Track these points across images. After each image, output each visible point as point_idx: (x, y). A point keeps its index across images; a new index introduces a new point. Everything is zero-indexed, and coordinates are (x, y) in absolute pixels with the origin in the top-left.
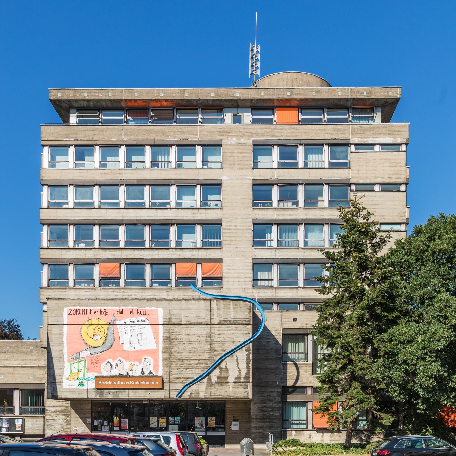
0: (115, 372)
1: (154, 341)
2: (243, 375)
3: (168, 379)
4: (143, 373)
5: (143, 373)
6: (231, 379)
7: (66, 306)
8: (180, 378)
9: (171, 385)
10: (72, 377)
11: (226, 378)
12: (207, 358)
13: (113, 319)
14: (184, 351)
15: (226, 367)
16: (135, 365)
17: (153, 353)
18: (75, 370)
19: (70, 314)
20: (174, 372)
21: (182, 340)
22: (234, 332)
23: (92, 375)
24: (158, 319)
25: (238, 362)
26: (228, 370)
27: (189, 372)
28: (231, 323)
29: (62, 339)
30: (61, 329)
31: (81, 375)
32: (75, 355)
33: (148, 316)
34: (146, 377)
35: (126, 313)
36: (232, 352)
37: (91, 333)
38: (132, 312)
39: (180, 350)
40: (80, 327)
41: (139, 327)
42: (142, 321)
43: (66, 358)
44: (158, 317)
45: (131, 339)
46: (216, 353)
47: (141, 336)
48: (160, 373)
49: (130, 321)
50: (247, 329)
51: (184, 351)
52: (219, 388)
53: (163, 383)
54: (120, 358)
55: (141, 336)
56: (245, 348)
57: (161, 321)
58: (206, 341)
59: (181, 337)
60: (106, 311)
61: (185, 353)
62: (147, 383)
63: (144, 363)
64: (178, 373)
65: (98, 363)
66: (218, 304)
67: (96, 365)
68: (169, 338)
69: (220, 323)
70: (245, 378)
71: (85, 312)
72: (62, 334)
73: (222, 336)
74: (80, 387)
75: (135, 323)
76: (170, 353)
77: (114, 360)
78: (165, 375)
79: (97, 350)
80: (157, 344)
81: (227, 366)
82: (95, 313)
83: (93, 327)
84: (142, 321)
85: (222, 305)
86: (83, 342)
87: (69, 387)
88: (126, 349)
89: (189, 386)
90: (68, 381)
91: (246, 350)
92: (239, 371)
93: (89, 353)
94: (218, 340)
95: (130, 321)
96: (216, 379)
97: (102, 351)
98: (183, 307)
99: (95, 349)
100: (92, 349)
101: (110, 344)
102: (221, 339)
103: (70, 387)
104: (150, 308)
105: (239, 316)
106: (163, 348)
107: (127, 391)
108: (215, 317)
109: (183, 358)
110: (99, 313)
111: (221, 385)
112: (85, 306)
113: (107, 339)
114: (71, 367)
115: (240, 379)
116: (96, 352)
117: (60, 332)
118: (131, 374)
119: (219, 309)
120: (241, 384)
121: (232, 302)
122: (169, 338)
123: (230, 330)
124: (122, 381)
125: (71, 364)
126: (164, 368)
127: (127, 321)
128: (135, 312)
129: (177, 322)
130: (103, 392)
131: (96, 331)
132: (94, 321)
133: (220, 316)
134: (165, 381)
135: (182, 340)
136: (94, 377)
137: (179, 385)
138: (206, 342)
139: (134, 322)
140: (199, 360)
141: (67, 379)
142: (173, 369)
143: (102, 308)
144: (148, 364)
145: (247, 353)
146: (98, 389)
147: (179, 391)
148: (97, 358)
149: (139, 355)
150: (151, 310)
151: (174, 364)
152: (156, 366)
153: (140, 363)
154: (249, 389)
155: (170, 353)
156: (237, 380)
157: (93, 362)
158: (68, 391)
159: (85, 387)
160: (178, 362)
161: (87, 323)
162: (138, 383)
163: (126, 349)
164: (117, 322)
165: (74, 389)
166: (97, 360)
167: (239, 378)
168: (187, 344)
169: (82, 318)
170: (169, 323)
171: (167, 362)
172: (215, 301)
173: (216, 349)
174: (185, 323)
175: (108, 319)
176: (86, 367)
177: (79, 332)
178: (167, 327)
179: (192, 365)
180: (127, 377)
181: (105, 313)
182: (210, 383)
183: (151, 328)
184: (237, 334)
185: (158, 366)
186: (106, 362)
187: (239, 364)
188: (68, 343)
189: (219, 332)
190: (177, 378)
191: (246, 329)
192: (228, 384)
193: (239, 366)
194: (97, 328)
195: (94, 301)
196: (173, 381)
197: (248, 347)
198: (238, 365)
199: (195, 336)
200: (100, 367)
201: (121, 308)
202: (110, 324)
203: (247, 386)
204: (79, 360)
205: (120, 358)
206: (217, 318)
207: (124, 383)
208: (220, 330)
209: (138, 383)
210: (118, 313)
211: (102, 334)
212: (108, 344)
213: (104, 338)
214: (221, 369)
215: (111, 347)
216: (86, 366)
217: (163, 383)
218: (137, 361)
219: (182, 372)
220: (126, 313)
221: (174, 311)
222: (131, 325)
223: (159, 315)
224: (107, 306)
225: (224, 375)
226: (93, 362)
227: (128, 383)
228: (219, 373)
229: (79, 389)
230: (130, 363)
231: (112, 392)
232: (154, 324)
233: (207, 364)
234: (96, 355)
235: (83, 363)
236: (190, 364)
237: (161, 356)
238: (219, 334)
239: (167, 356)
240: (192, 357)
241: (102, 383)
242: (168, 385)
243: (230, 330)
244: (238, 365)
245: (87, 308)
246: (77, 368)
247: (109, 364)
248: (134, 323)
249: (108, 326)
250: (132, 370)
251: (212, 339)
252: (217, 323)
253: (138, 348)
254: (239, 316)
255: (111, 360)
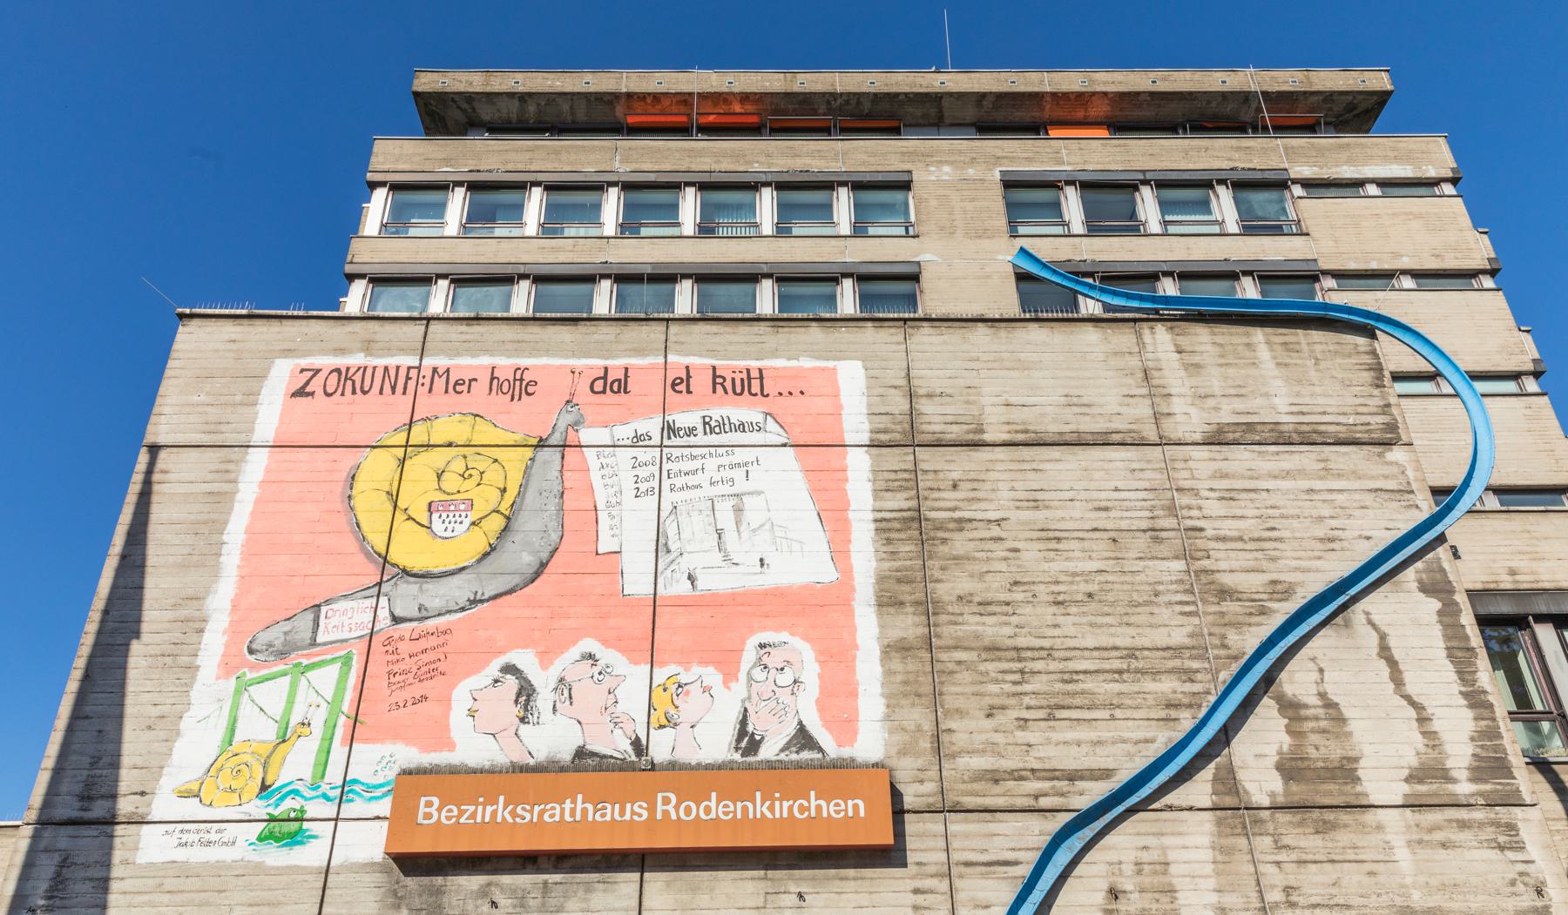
0: (552, 737)
1: (816, 538)
2: (1460, 752)
3: (930, 787)
4: (747, 741)
5: (747, 741)
6: (1382, 781)
7: (288, 353)
8: (1017, 776)
9: (958, 825)
10: (225, 780)
11: (1346, 771)
12: (1179, 637)
13: (567, 419)
14: (1019, 596)
15: (1322, 695)
16: (695, 689)
17: (815, 609)
18: (257, 729)
19: (301, 393)
20: (968, 730)
21: (996, 531)
22: (1318, 485)
23: (378, 760)
24: (837, 414)
25: (1392, 663)
26: (1341, 720)
27: (1070, 735)
28: (1282, 438)
29: (219, 526)
30: (229, 475)
31: (296, 765)
32: (287, 626)
33: (774, 404)
34: (770, 765)
35: (647, 386)
36: (1336, 601)
37: (415, 497)
38: (682, 383)
39: (995, 587)
40: (348, 459)
41: (725, 460)
42: (741, 427)
43: (213, 644)
44: (840, 407)
45: (671, 530)
46: (1230, 607)
47: (738, 510)
48: (870, 744)
49: (670, 430)
50: (1395, 470)
51: (1018, 596)
52: (1312, 843)
53: (899, 812)
54: (589, 645)
55: (738, 510)
56: (1410, 574)
57: (856, 426)
58: (1154, 533)
59: (992, 515)
60: (527, 377)
61: (1028, 609)
62: (783, 808)
63: (758, 674)
64: (999, 738)
65: (432, 673)
66: (1184, 341)
67: (417, 690)
68: (916, 518)
69: (1217, 439)
70: (1477, 774)
71: (393, 381)
72: (222, 500)
73: (1246, 507)
74: (276, 856)
75: (701, 439)
76: (929, 609)
77: (546, 657)
78: (902, 752)
79: (437, 595)
80: (840, 552)
81: (1329, 688)
82: (459, 386)
83: (437, 458)
84: (741, 427)
85: (1209, 347)
86: (352, 545)
87: (181, 855)
88: (637, 582)
89: (1088, 833)
90: (192, 809)
91: (1426, 589)
92: (1423, 720)
93: (383, 614)
94: (1229, 528)
95: (670, 430)
96: (1276, 783)
97: (474, 602)
98: (985, 357)
99: (430, 586)
100: (408, 588)
101: (533, 560)
102: (1249, 527)
103: (197, 855)
104: (793, 363)
105: (1321, 400)
106: (881, 579)
107: (627, 882)
108: (1177, 405)
109: (1022, 642)
110: (482, 386)
111: (1324, 828)
112: (402, 351)
113: (515, 525)
114: (236, 707)
115: (1445, 776)
116: (435, 604)
117: (215, 487)
118: (660, 751)
119: (1197, 366)
120: (1463, 814)
121: (1259, 335)
122: (916, 518)
123: (1287, 475)
124: (597, 800)
125: (243, 688)
126: (893, 702)
127: (652, 426)
128: (701, 382)
129: (955, 432)
130: (439, 892)
131: (451, 482)
132: (444, 429)
133: (1211, 402)
134: (909, 801)
135: (996, 531)
136: (391, 775)
137: (1010, 825)
138: (1156, 539)
139: (691, 431)
140: (1132, 653)
141: (185, 794)
142: (960, 713)
143: (505, 364)
144: (786, 679)
145: (1435, 605)
146: (410, 863)
147: (1025, 871)
148: (433, 641)
149: (713, 626)
150: (798, 374)
151: (965, 676)
152: (838, 696)
153: (729, 676)
154: (1533, 851)
155: (929, 609)
156: (1428, 790)
157: (401, 670)
158: (170, 884)
159: (311, 855)
160: (991, 667)
161: (400, 438)
162: (716, 808)
163: (637, 582)
164: (586, 435)
165: (218, 868)
166: (426, 658)
167: (1430, 771)
168: (1032, 555)
169: (377, 415)
170: (904, 437)
171: (911, 666)
172: (1160, 328)
173: (1227, 580)
174: (1005, 437)
175: (537, 416)
176: (347, 705)
177: (339, 488)
178: (897, 460)
179: (1088, 684)
180: (638, 765)
181: (520, 386)
182: (1233, 808)
183: (795, 465)
184: (1340, 498)
185: (854, 694)
186: (493, 669)
187: (1408, 677)
188: (249, 553)
189: (1225, 484)
190: (995, 777)
191: (1387, 470)
192: (1370, 817)
193: (1410, 689)
194: (459, 466)
195: (463, 328)
196: (970, 802)
197: (1428, 570)
198: (1397, 679)
199: (1078, 510)
200: (446, 701)
201: (617, 363)
202: (541, 444)
203: (1511, 828)
204: (296, 658)
205: (589, 645)
206: (1193, 411)
207: (611, 812)
208: (1224, 476)
209: (716, 808)
210: (599, 386)
211: (486, 498)
212: (519, 557)
213: (497, 523)
214: (1291, 708)
215: (538, 574)
216: (350, 695)
217: (899, 812)
218: (704, 662)
219: (1021, 736)
220: (647, 386)
221: (926, 378)
222: (676, 452)
223: (844, 400)
224: (535, 352)
225: (1322, 750)
226: (401, 670)
227: (638, 811)
228: (1286, 741)
229: (259, 869)
230: (661, 675)
231: (512, 892)
232: (817, 447)
233: (1188, 675)
234: (431, 623)
235: (325, 678)
236: (1070, 677)
237: (867, 627)
238: (1228, 497)
239: (908, 625)
240: (1075, 630)
241: (442, 822)
242: (934, 824)
243: (1287, 475)
244: (1397, 679)
245: (413, 361)
246: (277, 710)
247: (511, 682)
248: (692, 440)
249: (529, 452)
250: (670, 722)
251: (1190, 523)
252: (1198, 437)
253: (715, 581)
254: (1321, 400)
255: (525, 659)
